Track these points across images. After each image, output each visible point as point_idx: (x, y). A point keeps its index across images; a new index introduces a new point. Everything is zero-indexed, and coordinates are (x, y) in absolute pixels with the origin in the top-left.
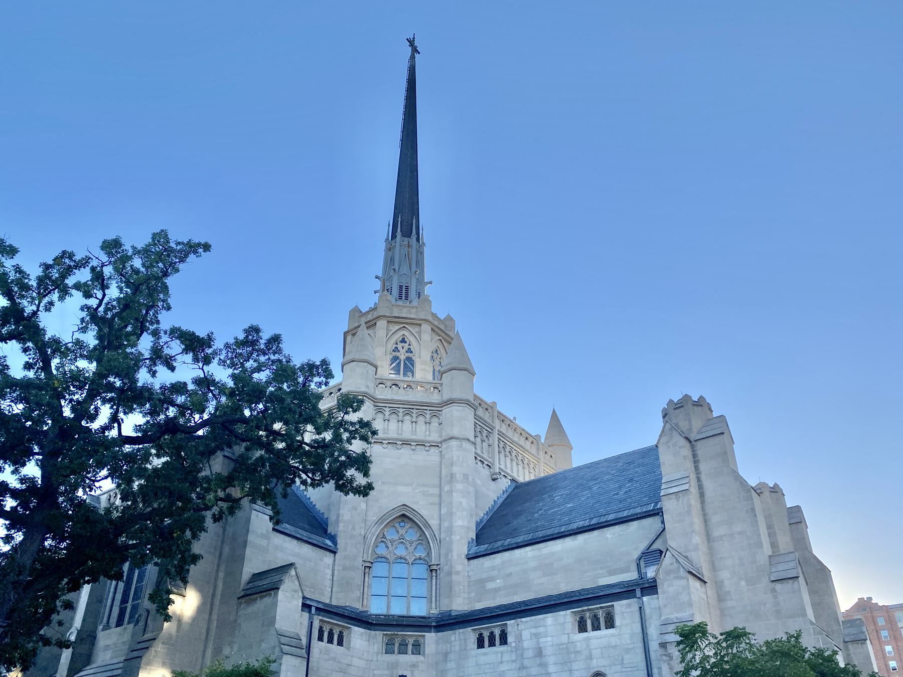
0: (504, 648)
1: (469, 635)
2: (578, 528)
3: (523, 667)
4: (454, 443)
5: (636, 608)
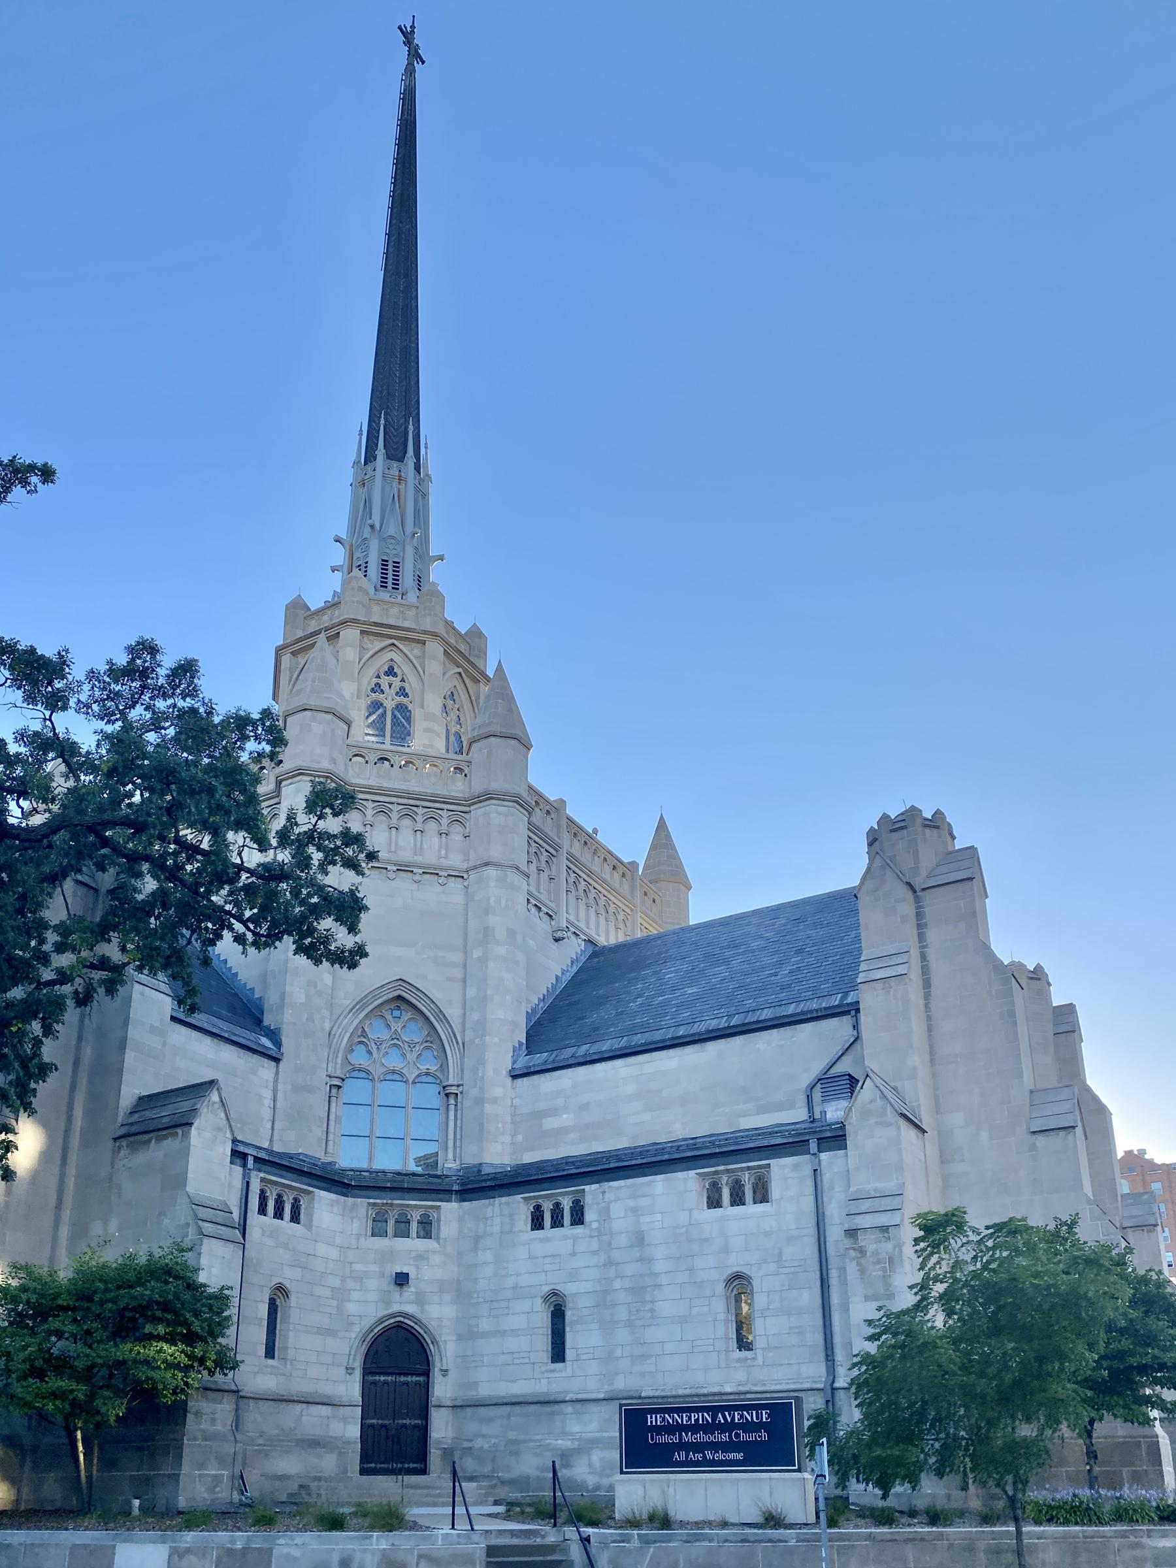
0: (579, 1230)
1: (518, 1206)
2: (708, 1031)
3: (610, 1263)
4: (492, 872)
5: (807, 1171)
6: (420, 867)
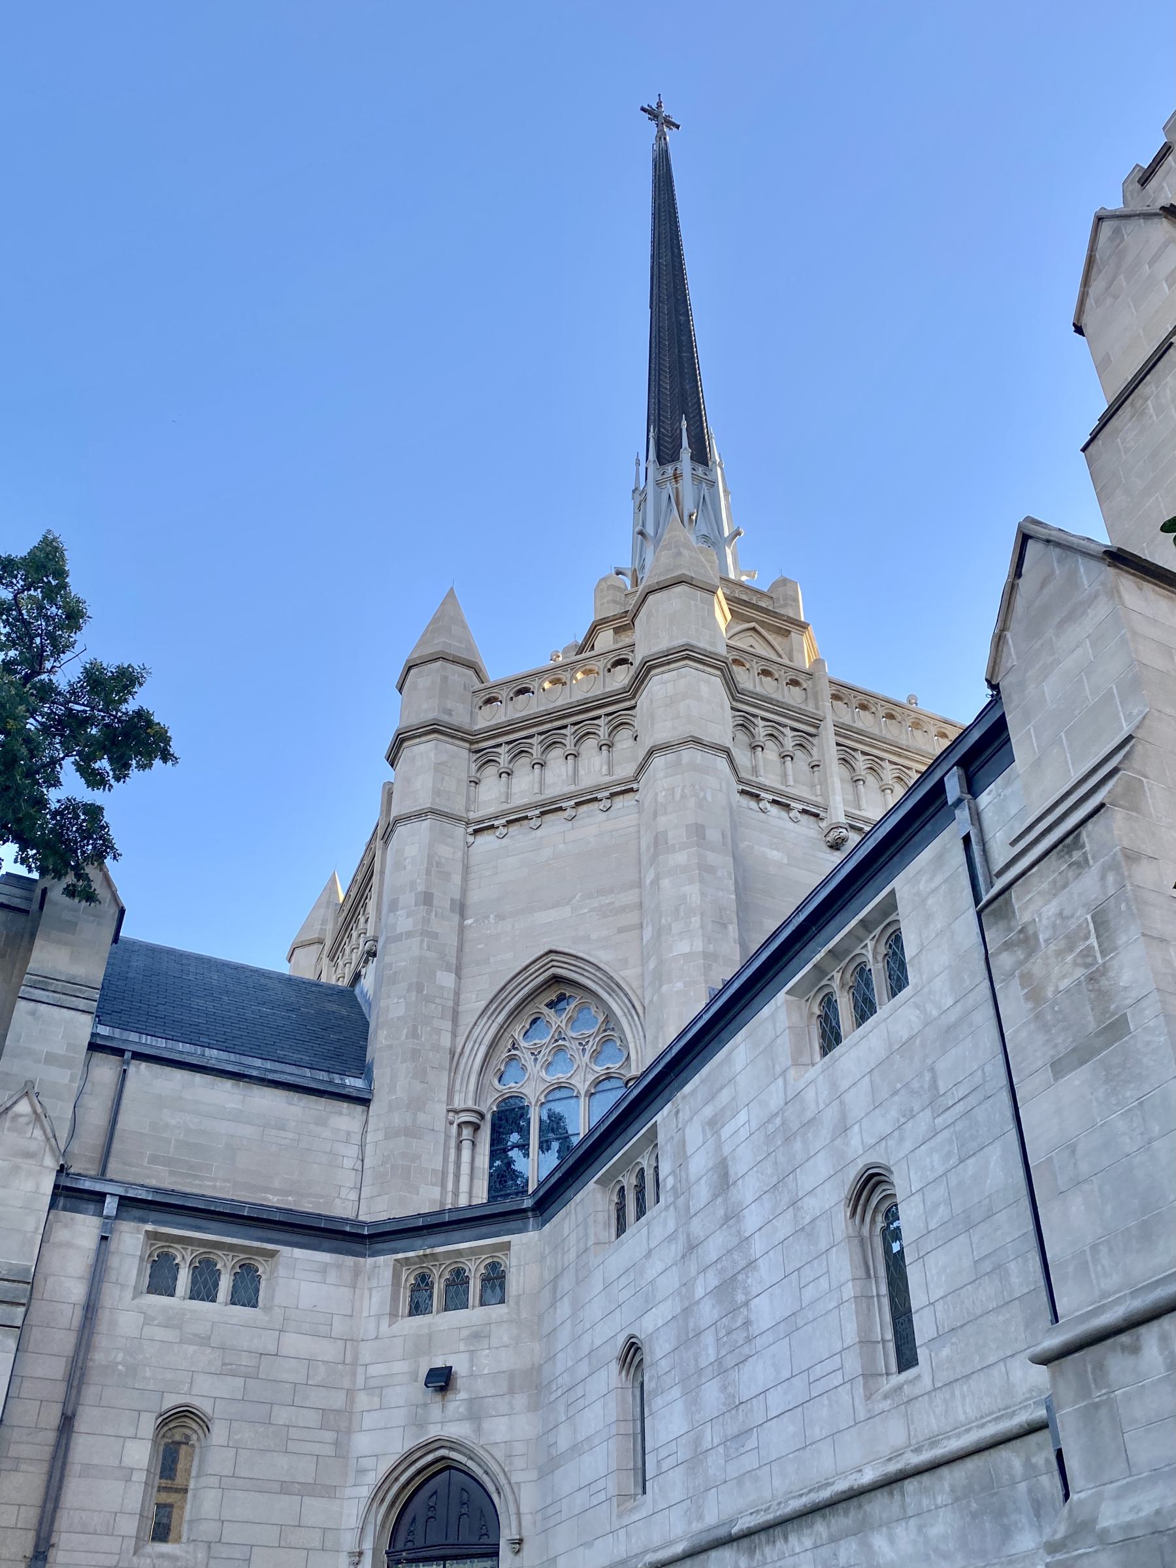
6: (570, 798)
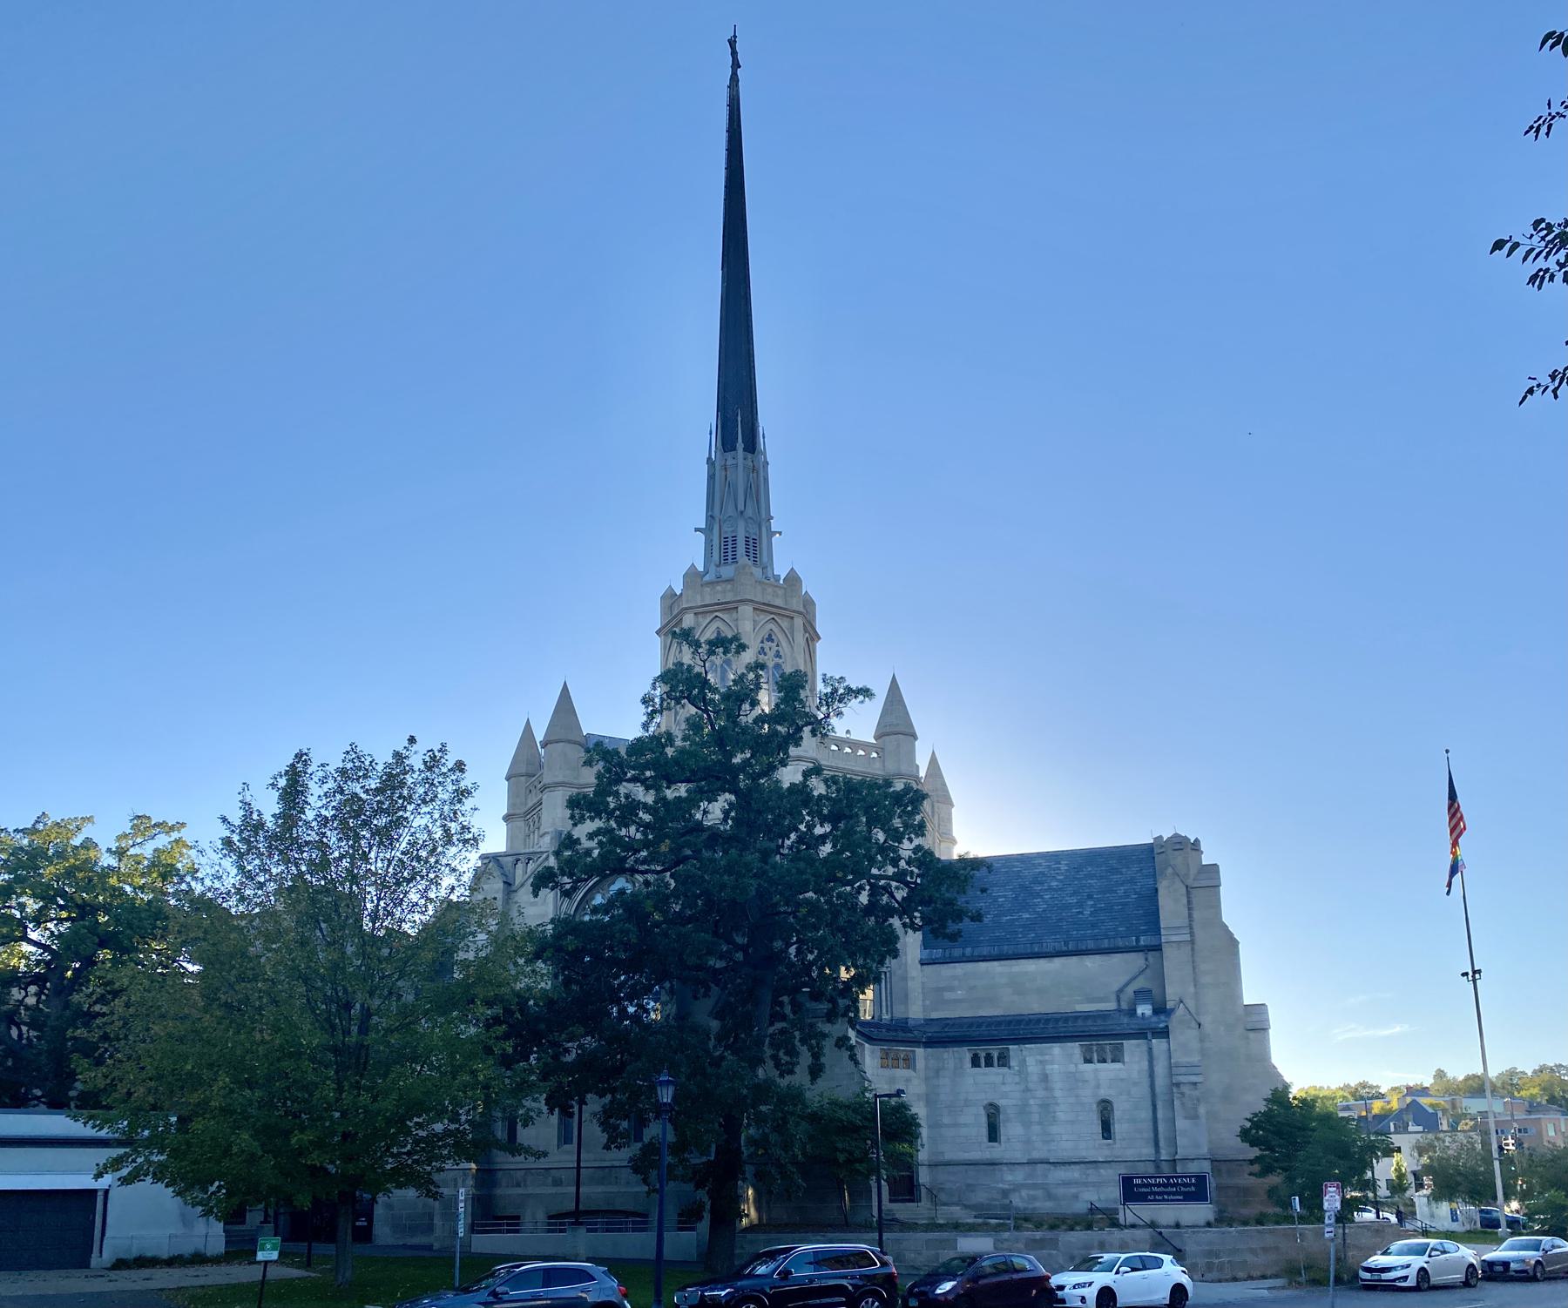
0: (1005, 1070)
1: (965, 1053)
3: (1027, 1090)
5: (1145, 1048)
